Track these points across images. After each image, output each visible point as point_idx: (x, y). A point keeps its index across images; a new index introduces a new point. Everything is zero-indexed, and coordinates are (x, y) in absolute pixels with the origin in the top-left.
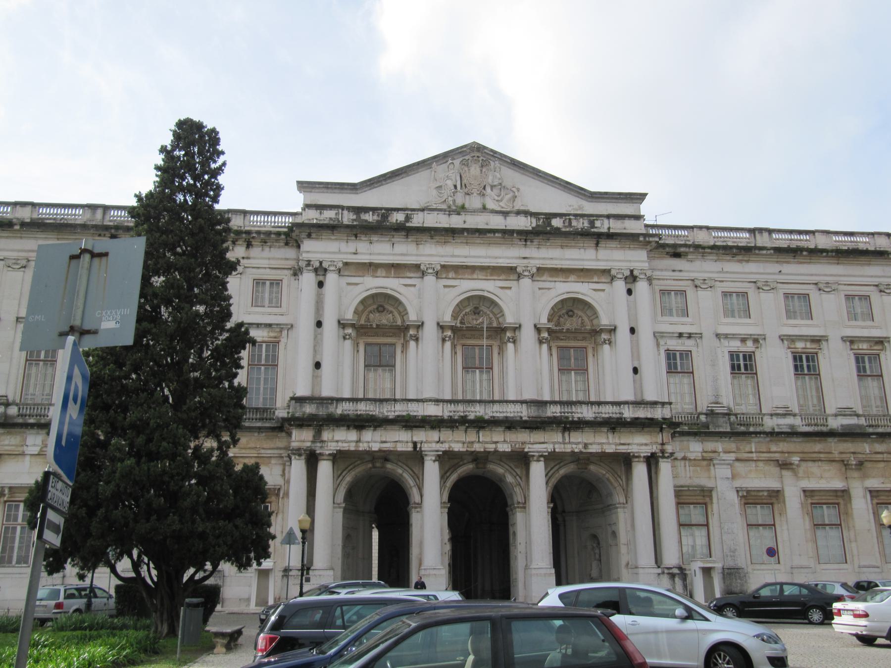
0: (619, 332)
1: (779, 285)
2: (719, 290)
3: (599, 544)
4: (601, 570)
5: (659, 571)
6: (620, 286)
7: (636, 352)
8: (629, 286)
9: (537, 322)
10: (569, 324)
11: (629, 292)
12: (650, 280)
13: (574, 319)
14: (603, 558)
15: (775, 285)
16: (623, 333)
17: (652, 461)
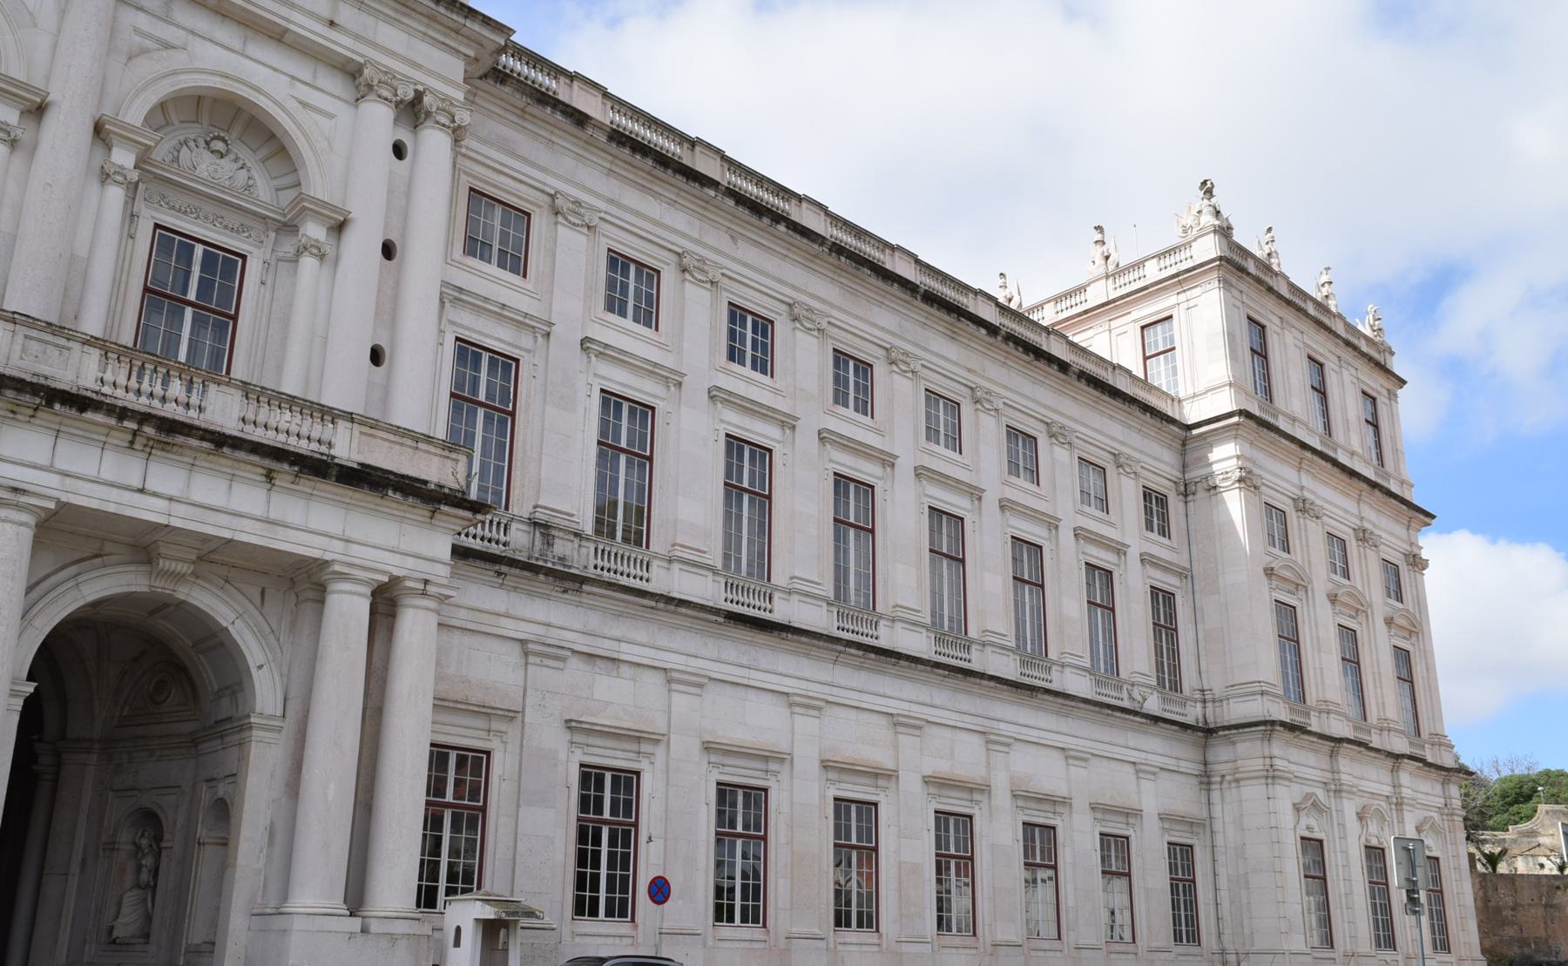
0: (352, 237)
1: (726, 281)
2: (604, 244)
3: (158, 838)
4: (148, 919)
5: (355, 924)
6: (379, 119)
7: (389, 307)
8: (404, 136)
9: (108, 111)
10: (205, 167)
11: (399, 151)
12: (457, 134)
13: (226, 165)
14: (167, 881)
15: (718, 277)
16: (361, 245)
17: (385, 602)
